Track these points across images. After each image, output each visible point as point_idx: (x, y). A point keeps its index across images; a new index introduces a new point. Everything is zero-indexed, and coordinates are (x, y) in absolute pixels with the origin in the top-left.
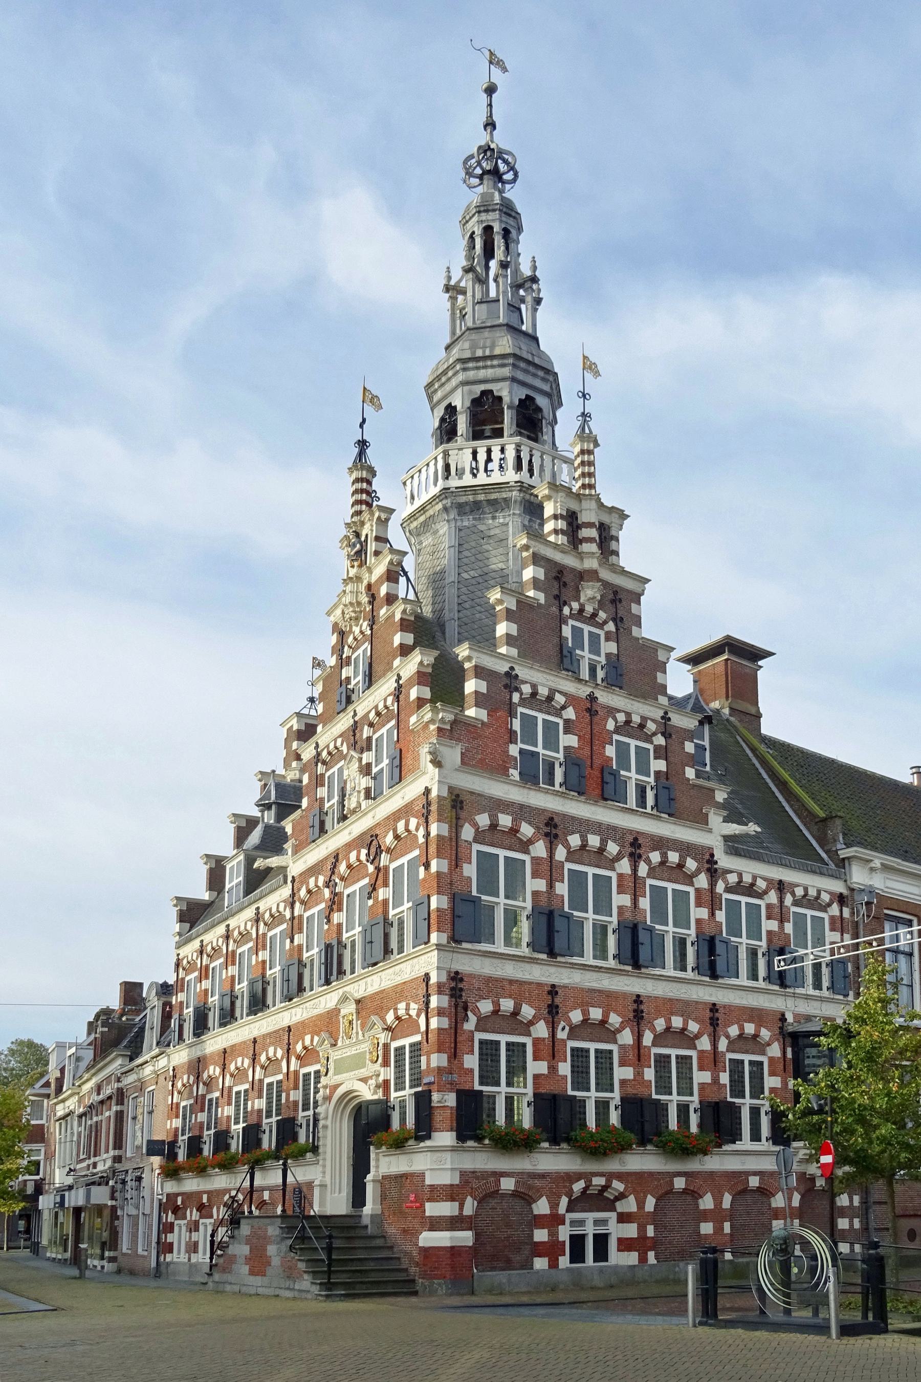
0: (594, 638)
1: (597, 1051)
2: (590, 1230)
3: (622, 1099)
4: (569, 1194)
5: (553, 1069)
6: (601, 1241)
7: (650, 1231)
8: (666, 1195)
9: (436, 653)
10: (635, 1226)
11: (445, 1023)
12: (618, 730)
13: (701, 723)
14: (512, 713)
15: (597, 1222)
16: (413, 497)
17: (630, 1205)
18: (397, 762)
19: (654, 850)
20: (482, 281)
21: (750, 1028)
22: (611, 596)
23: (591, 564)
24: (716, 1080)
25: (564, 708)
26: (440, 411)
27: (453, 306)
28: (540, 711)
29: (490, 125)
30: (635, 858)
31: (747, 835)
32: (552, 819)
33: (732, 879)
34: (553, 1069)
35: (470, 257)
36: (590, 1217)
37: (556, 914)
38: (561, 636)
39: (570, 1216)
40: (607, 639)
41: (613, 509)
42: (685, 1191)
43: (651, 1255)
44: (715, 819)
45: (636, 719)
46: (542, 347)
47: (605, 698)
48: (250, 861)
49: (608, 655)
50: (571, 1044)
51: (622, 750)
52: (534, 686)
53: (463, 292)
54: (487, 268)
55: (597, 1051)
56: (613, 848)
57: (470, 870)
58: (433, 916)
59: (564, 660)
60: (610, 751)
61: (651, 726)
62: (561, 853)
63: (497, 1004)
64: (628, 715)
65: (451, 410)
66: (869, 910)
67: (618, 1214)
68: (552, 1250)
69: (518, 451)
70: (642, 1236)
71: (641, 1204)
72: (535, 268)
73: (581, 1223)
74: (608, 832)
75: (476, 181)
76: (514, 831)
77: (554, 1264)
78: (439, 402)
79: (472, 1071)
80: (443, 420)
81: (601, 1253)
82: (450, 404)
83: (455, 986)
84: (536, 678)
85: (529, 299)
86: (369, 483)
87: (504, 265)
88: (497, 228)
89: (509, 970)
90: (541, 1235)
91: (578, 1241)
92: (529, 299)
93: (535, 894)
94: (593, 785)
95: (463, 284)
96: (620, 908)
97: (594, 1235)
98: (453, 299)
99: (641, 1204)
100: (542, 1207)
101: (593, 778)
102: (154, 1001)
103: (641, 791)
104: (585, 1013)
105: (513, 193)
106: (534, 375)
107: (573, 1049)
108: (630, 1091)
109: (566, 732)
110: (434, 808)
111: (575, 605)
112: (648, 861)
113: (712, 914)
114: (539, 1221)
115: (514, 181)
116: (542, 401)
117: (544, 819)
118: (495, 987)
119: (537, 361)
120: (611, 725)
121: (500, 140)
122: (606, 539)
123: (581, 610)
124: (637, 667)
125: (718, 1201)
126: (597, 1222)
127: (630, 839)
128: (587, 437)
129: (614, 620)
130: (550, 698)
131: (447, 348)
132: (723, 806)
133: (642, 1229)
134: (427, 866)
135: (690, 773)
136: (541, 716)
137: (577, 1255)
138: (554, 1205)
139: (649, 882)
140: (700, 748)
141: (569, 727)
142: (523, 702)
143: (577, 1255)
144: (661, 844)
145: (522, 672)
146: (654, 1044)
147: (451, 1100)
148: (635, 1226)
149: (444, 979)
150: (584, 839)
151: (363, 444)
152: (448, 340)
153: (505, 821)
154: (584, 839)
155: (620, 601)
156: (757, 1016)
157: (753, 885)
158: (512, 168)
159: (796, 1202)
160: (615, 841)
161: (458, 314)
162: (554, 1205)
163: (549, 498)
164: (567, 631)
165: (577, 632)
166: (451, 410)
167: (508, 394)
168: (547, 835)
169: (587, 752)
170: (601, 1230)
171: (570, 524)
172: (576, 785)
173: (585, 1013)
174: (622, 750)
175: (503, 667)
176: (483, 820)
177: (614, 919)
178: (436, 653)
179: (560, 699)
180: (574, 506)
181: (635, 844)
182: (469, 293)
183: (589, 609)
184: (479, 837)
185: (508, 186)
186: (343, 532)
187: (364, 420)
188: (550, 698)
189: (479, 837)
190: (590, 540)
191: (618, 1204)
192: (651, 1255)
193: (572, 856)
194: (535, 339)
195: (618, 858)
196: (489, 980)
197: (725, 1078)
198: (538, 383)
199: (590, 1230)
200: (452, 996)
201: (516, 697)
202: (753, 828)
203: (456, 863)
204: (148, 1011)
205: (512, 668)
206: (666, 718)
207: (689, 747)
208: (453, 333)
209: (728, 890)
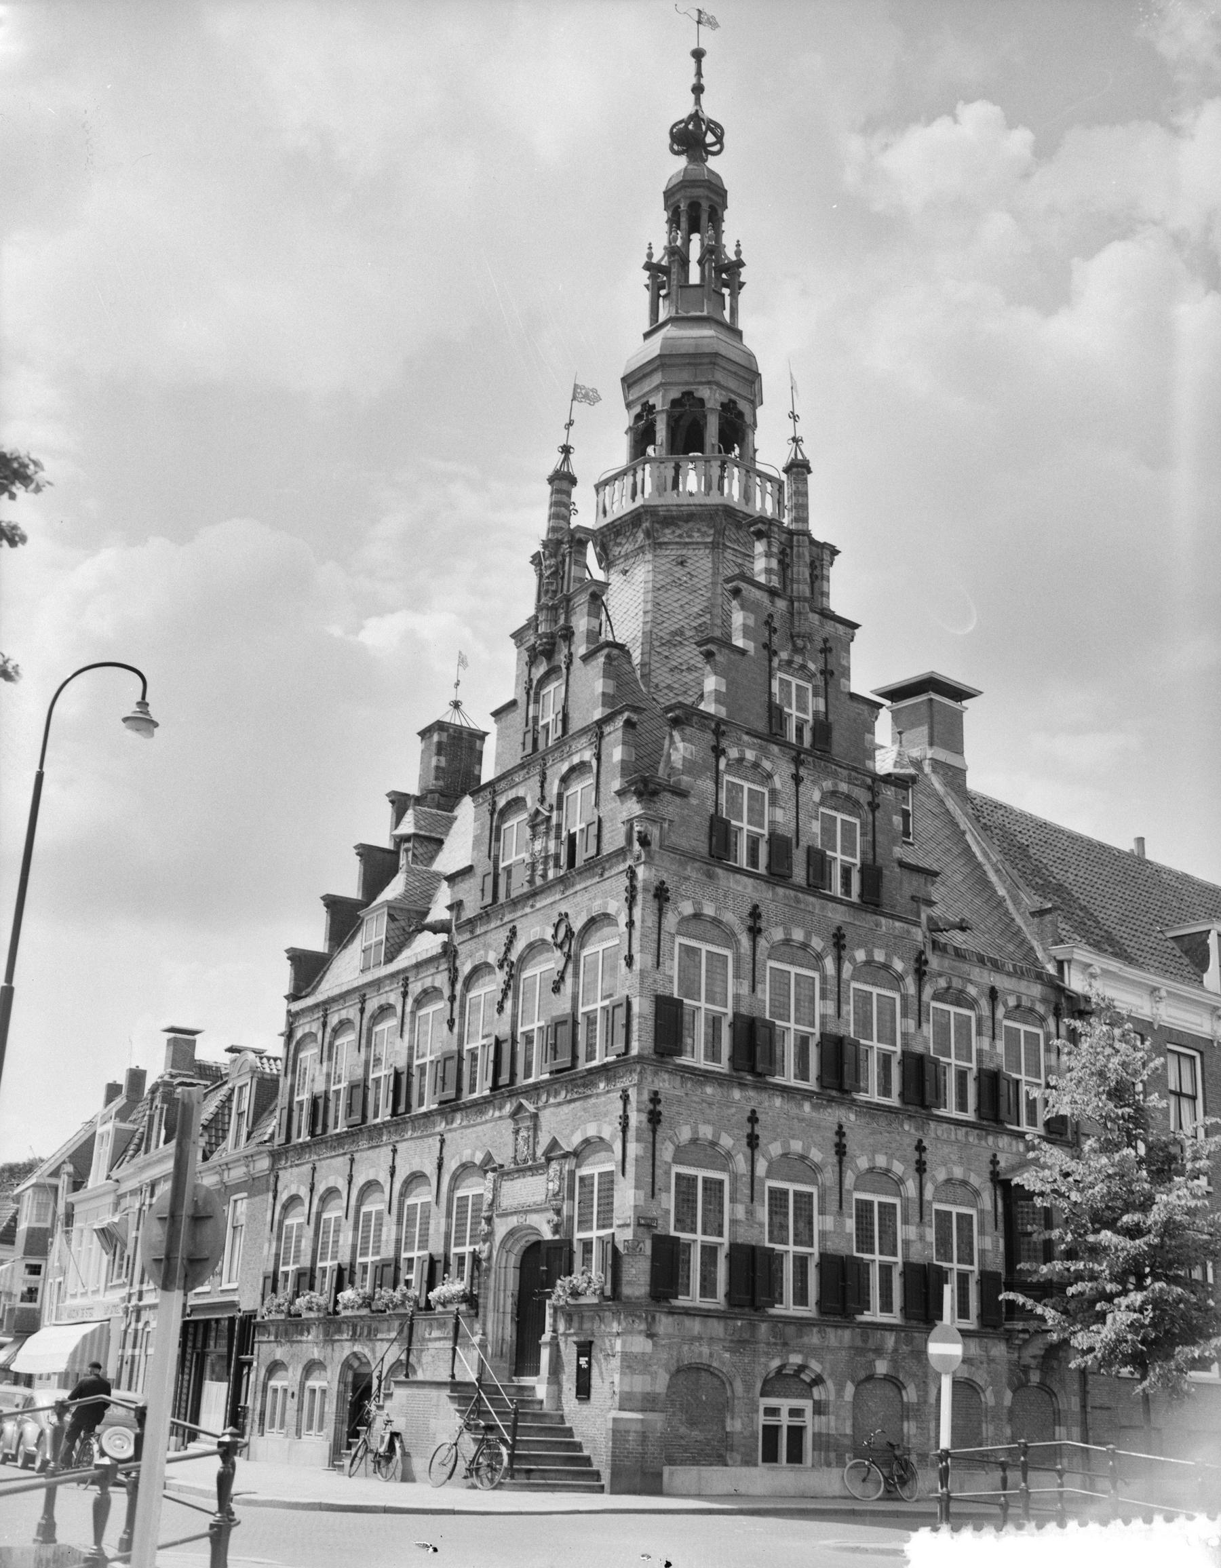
1: (796, 1193)
2: (785, 1421)
6: (796, 1433)
19: (859, 946)
20: (685, 263)
36: (785, 1404)
37: (758, 1024)
40: (815, 695)
41: (824, 546)
49: (816, 713)
60: (816, 827)
65: (649, 409)
67: (815, 1402)
72: (738, 253)
80: (638, 417)
88: (705, 205)
91: (771, 1433)
97: (789, 1427)
126: (795, 1412)
131: (647, 335)
152: (646, 327)
155: (830, 650)
160: (818, 935)
165: (785, 684)
167: (712, 398)
170: (796, 1422)
182: (674, 277)
191: (815, 1390)
199: (785, 1421)
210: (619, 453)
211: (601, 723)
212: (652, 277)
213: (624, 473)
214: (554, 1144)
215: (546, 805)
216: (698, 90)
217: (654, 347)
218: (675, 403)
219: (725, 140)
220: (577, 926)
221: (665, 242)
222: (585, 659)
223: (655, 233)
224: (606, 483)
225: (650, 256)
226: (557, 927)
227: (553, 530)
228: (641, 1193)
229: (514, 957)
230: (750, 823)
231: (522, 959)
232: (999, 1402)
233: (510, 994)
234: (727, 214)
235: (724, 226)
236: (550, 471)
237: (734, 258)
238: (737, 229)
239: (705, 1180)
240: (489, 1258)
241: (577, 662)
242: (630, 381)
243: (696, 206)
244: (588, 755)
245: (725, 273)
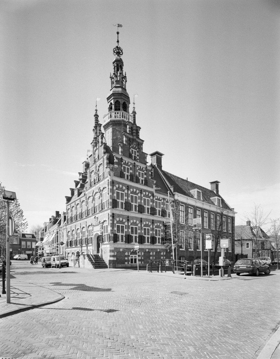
0: (135, 152)
1: (135, 227)
2: (134, 258)
3: (139, 236)
4: (131, 252)
5: (128, 230)
6: (135, 259)
7: (143, 258)
8: (145, 252)
9: (109, 154)
10: (140, 257)
11: (112, 222)
12: (139, 170)
13: (152, 168)
14: (122, 166)
15: (135, 257)
16: (105, 122)
17: (140, 254)
18: (103, 174)
19: (144, 192)
20: (116, 76)
21: (158, 224)
22: (138, 144)
23: (135, 137)
24: (153, 233)
25: (130, 165)
26: (109, 104)
27: (112, 81)
28: (126, 166)
29: (118, 42)
30: (141, 193)
31: (159, 190)
32: (128, 186)
33: (156, 197)
34: (128, 230)
35: (114, 71)
36: (134, 256)
38: (130, 151)
39: (131, 255)
42: (148, 252)
43: (143, 262)
44: (154, 186)
45: (142, 168)
46: (127, 91)
47: (137, 163)
48: (79, 190)
50: (131, 226)
51: (139, 173)
52: (125, 161)
53: (113, 78)
54: (117, 73)
55: (135, 227)
56: (138, 191)
57: (115, 195)
58: (110, 203)
59: (130, 156)
60: (137, 173)
61: (144, 169)
62: (129, 192)
63: (119, 219)
64: (140, 167)
65: (111, 104)
66: (177, 203)
68: (128, 261)
69: (123, 113)
70: (142, 259)
71: (141, 254)
72: (125, 74)
73: (132, 257)
74: (137, 188)
75: (115, 54)
76: (122, 188)
77: (128, 263)
79: (116, 230)
80: (110, 106)
81: (135, 262)
83: (113, 216)
84: (126, 160)
85: (124, 80)
86: (98, 118)
87: (120, 74)
89: (121, 213)
90: (126, 258)
91: (132, 259)
92: (124, 80)
93: (125, 199)
94: (135, 180)
95: (113, 77)
96: (139, 202)
97: (134, 259)
98: (111, 80)
99: (141, 254)
100: (126, 254)
101: (134, 178)
102: (62, 216)
103: (142, 181)
104: (133, 221)
105: (122, 57)
106: (126, 98)
107: (131, 227)
108: (140, 234)
109: (131, 169)
111: (132, 145)
112: (143, 194)
113: (153, 204)
114: (126, 256)
115: (122, 54)
116: (127, 103)
117: (127, 186)
118: (119, 216)
119: (126, 95)
120: (137, 169)
121: (120, 46)
123: (133, 147)
124: (143, 157)
125: (153, 253)
126: (135, 257)
127: (140, 190)
128: (134, 113)
129: (138, 149)
130: (128, 163)
131: (111, 90)
132: (155, 184)
133: (141, 258)
134: (108, 194)
135: (150, 178)
136: (126, 167)
137: (132, 262)
138: (128, 254)
139: (143, 198)
140: (152, 173)
141: (131, 169)
142: (123, 164)
143: (132, 262)
144: (145, 191)
145: (123, 158)
146: (144, 226)
147: (113, 235)
148: (140, 257)
149: (111, 214)
150: (133, 190)
151: (96, 110)
153: (121, 186)
154: (133, 190)
156: (160, 222)
157: (159, 199)
158: (122, 52)
159: (165, 254)
161: (112, 83)
162: (128, 254)
163: (128, 124)
164: (131, 151)
165: (132, 151)
166: (111, 104)
167: (122, 102)
168: (127, 189)
169: (134, 173)
171: (131, 129)
172: (132, 180)
173: (133, 221)
174: (139, 173)
175: (120, 157)
176: (117, 186)
177: (138, 204)
178: (109, 154)
179: (129, 164)
180: (132, 126)
181: (141, 191)
183: (134, 146)
184: (117, 189)
185: (121, 55)
186: (94, 128)
187: (96, 106)
188: (128, 163)
189: (117, 189)
190: (134, 133)
192: (143, 262)
193: (131, 193)
194: (126, 90)
195: (138, 193)
196: (118, 215)
197: (154, 232)
198: (126, 99)
199: (134, 258)
200: (113, 217)
201: (122, 163)
202: (160, 189)
203: (113, 194)
204: (61, 218)
205: (122, 157)
206: (146, 167)
207: (150, 173)
208: (112, 87)
209: (156, 199)
210: (107, 111)
214: (100, 222)
217: (111, 92)
219: (123, 51)
222: (101, 146)
223: (111, 70)
225: (111, 75)
227: (96, 125)
228: (112, 228)
230: (127, 172)
232: (163, 254)
237: (125, 75)
238: (126, 69)
239: (121, 226)
243: (119, 65)
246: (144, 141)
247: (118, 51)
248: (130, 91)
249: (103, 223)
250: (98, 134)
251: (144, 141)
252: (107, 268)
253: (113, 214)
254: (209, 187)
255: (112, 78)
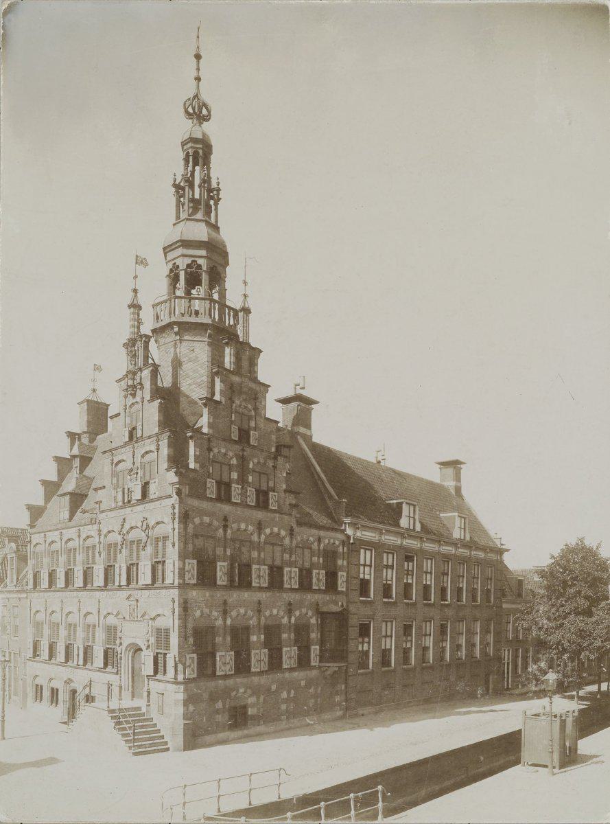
20: (191, 186)
26: (170, 265)
65: (176, 267)
78: (169, 261)
80: (171, 271)
82: (175, 263)
95: (182, 184)
105: (210, 129)
110: (177, 516)
122: (253, 363)
151: (135, 291)
194: (218, 228)
211: (157, 435)
212: (177, 192)
213: (165, 301)
215: (136, 465)
216: (198, 69)
218: (189, 266)
220: (151, 525)
221: (182, 172)
224: (157, 304)
225: (175, 180)
226: (142, 522)
229: (125, 531)
231: (128, 532)
233: (124, 546)
234: (212, 157)
235: (211, 165)
236: (129, 302)
237: (216, 186)
240: (121, 654)
241: (146, 402)
242: (167, 250)
243: (199, 153)
244: (153, 448)
245: (212, 194)
246: (269, 386)
247: (198, 112)
248: (229, 235)
249: (154, 619)
250: (140, 362)
251: (269, 386)
252: (168, 749)
253: (186, 602)
254: (433, 475)
255: (177, 187)
